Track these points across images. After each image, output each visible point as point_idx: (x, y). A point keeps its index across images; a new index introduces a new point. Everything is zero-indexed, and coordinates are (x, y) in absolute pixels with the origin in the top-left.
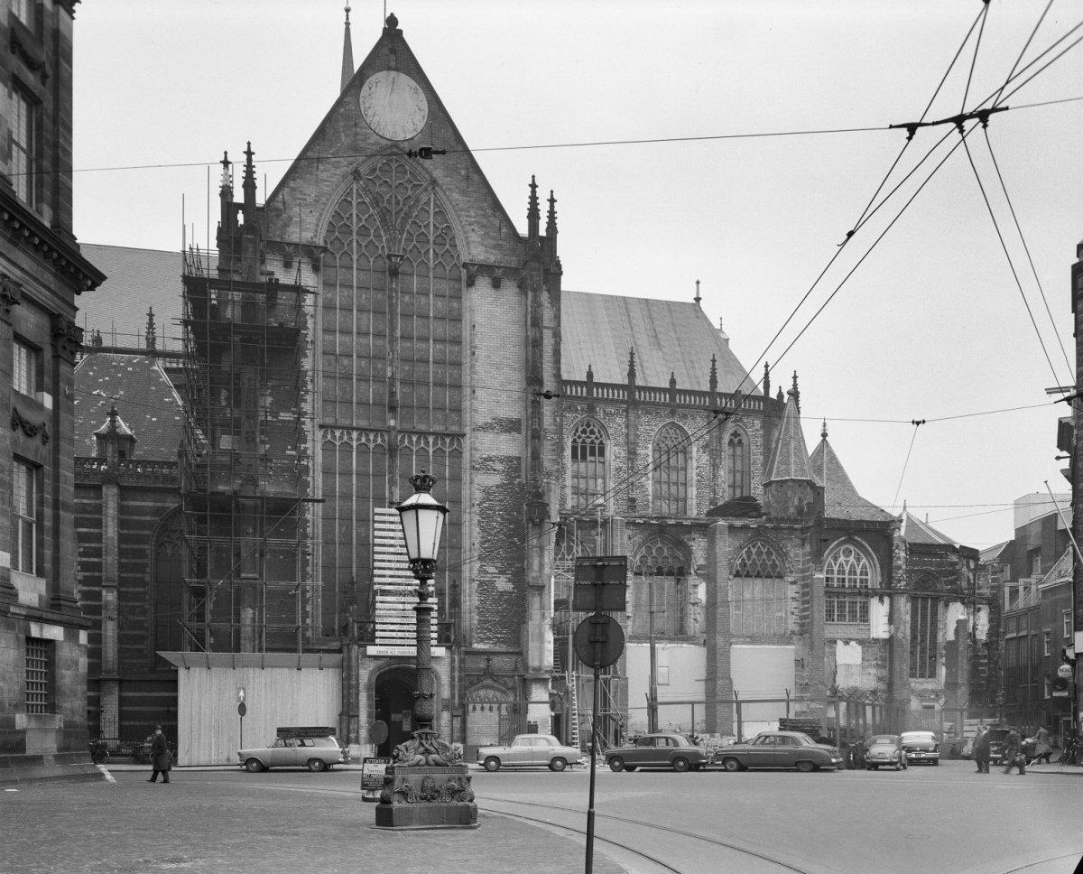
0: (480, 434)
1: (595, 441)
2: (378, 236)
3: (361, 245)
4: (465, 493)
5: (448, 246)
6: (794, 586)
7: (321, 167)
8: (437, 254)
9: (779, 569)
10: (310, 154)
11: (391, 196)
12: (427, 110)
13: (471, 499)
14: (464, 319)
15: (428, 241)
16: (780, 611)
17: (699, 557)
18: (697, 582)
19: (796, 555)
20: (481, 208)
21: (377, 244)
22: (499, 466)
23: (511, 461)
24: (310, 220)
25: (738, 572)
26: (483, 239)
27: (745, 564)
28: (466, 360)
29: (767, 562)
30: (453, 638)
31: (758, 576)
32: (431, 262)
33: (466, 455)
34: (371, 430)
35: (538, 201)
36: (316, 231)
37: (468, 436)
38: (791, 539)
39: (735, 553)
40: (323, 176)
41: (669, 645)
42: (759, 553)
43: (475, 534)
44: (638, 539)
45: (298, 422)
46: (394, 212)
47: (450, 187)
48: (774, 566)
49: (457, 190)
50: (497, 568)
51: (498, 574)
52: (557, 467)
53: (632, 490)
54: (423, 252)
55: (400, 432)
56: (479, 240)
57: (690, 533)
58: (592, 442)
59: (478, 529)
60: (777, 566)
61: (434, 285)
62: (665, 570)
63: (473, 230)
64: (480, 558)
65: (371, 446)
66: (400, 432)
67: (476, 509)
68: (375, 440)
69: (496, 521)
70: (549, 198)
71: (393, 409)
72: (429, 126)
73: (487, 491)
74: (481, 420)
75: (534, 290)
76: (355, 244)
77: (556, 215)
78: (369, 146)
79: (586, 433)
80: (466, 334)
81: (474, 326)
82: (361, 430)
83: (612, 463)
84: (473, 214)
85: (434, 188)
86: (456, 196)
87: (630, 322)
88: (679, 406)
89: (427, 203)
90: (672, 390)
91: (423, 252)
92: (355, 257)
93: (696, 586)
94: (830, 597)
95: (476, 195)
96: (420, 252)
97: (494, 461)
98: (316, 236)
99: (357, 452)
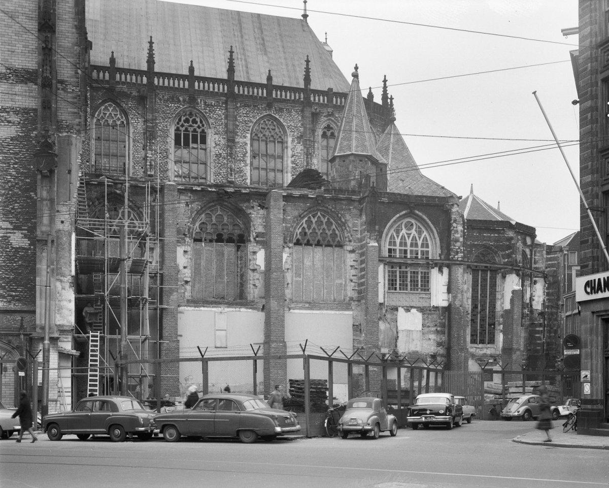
1: (197, 130)
6: (353, 255)
9: (339, 238)
16: (340, 277)
17: (258, 225)
18: (256, 249)
19: (355, 225)
22: (14, 118)
23: (27, 113)
25: (298, 240)
27: (306, 234)
29: (327, 232)
31: (318, 244)
38: (350, 209)
39: (294, 222)
42: (319, 223)
44: (196, 206)
48: (334, 235)
50: (11, 223)
51: (13, 229)
53: (231, 175)
57: (249, 202)
58: (195, 131)
60: (337, 235)
62: (225, 237)
69: (11, 175)
79: (188, 122)
83: (213, 149)
87: (241, 31)
88: (276, 100)
90: (269, 86)
93: (255, 253)
94: (392, 267)
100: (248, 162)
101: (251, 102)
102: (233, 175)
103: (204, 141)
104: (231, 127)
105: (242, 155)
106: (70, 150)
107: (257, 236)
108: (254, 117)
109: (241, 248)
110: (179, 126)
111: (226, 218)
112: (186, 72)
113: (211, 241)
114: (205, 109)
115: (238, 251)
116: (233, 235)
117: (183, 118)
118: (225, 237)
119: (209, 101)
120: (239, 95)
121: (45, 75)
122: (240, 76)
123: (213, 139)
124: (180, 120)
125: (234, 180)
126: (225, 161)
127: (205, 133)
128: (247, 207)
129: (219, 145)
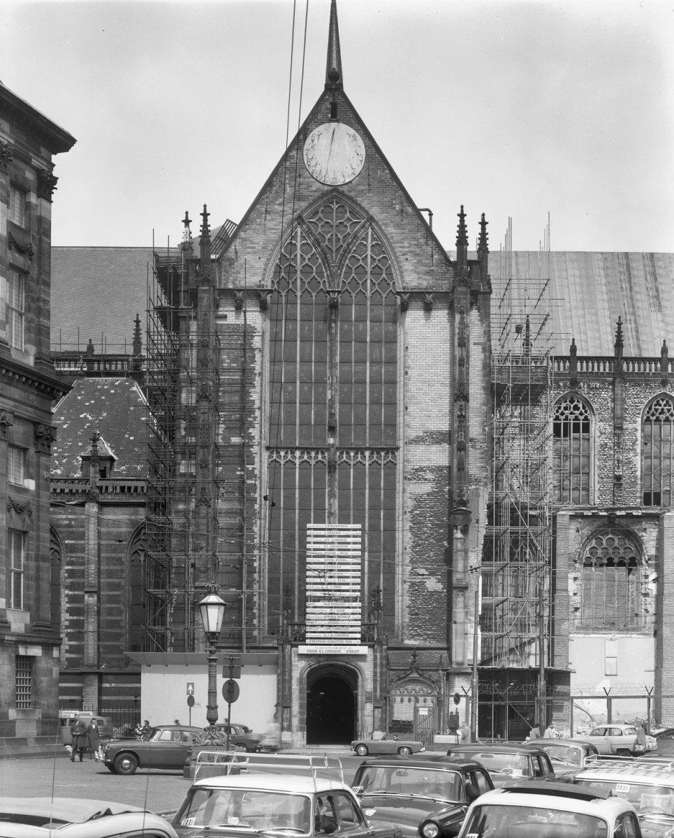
0: (412, 447)
2: (320, 274)
3: (304, 282)
4: (399, 501)
5: (384, 275)
7: (269, 217)
8: (374, 284)
10: (258, 206)
11: (332, 235)
12: (364, 154)
13: (403, 507)
14: (398, 341)
17: (650, 549)
20: (415, 239)
21: (319, 280)
22: (429, 476)
23: (441, 470)
24: (260, 265)
28: (400, 379)
30: (376, 637)
32: (369, 291)
33: (400, 467)
34: (313, 449)
35: (466, 229)
36: (264, 275)
37: (401, 449)
40: (270, 225)
41: (617, 636)
43: (407, 539)
44: (586, 532)
45: (245, 447)
46: (334, 250)
47: (385, 222)
51: (428, 575)
52: (485, 474)
54: (361, 283)
55: (338, 449)
56: (412, 268)
59: (410, 535)
61: (371, 310)
63: (407, 259)
64: (412, 562)
65: (313, 462)
66: (338, 449)
67: (408, 516)
68: (316, 457)
70: (480, 221)
71: (332, 429)
72: (366, 168)
73: (419, 500)
74: (412, 434)
75: (462, 313)
76: (299, 281)
77: (487, 236)
78: (311, 194)
80: (400, 354)
81: (407, 348)
82: (304, 450)
84: (408, 245)
89: (365, 239)
91: (361, 283)
92: (299, 294)
95: (409, 227)
96: (358, 283)
97: (425, 471)
98: (263, 279)
99: (300, 468)
100: (639, 451)
101: (642, 380)
102: (621, 468)
103: (586, 428)
104: (618, 412)
105: (631, 444)
106: (478, 501)
107: (649, 560)
108: (645, 397)
109: (633, 571)
110: (558, 414)
111: (617, 541)
112: (567, 353)
113: (601, 565)
114: (588, 393)
115: (629, 574)
116: (624, 558)
117: (563, 405)
118: (616, 560)
119: (593, 384)
120: (628, 374)
121: (460, 440)
122: (630, 351)
123: (598, 427)
124: (559, 408)
125: (621, 473)
126: (612, 452)
127: (589, 420)
128: (639, 530)
129: (604, 433)
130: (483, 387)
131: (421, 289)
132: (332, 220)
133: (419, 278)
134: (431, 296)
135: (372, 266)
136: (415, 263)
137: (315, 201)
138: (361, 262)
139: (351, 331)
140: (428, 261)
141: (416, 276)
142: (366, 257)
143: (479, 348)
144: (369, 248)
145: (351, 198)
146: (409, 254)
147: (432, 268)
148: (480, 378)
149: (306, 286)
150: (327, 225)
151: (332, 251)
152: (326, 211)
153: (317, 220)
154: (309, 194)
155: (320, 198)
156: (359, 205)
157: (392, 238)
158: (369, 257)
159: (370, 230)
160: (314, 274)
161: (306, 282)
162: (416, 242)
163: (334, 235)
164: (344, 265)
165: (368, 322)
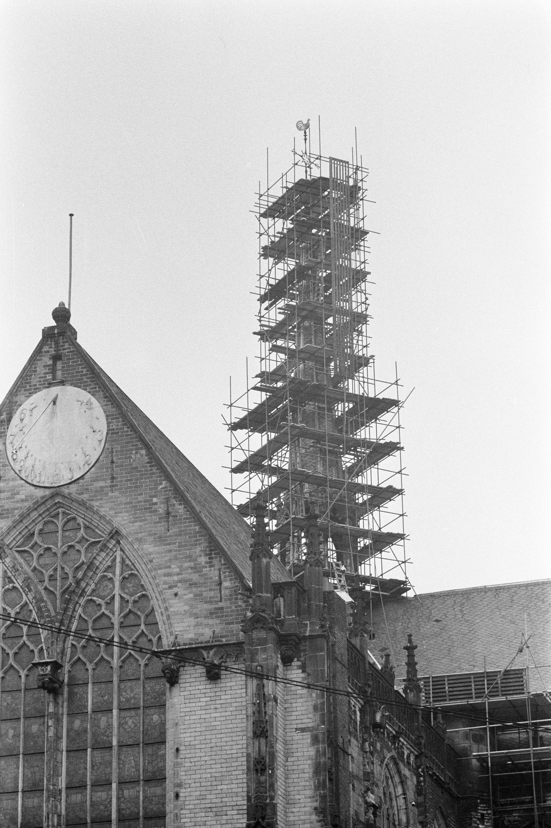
5: (143, 627)
11: (55, 570)
15: (112, 627)
20: (190, 558)
21: (32, 647)
26: (192, 606)
47: (140, 535)
49: (151, 539)
56: (187, 608)
63: (176, 595)
78: (18, 505)
81: (178, 750)
85: (118, 542)
86: (149, 548)
89: (111, 568)
95: (179, 539)
130: (316, 809)
131: (202, 643)
132: (56, 544)
133: (197, 625)
134: (212, 652)
135: (122, 615)
136: (191, 599)
137: (23, 517)
138: (103, 610)
139: (85, 731)
140: (212, 594)
141: (192, 621)
142: (113, 598)
143: (307, 736)
144: (117, 584)
145: (82, 504)
146: (179, 585)
147: (220, 605)
148: (309, 793)
149: (11, 661)
150: (48, 554)
151: (55, 596)
152: (46, 530)
153: (32, 548)
154: (13, 506)
155: (30, 511)
156: (97, 513)
157: (151, 561)
158: (117, 599)
159: (118, 553)
160: (25, 638)
161: (11, 653)
162: (192, 564)
163: (59, 569)
164: (72, 617)
165: (115, 712)
